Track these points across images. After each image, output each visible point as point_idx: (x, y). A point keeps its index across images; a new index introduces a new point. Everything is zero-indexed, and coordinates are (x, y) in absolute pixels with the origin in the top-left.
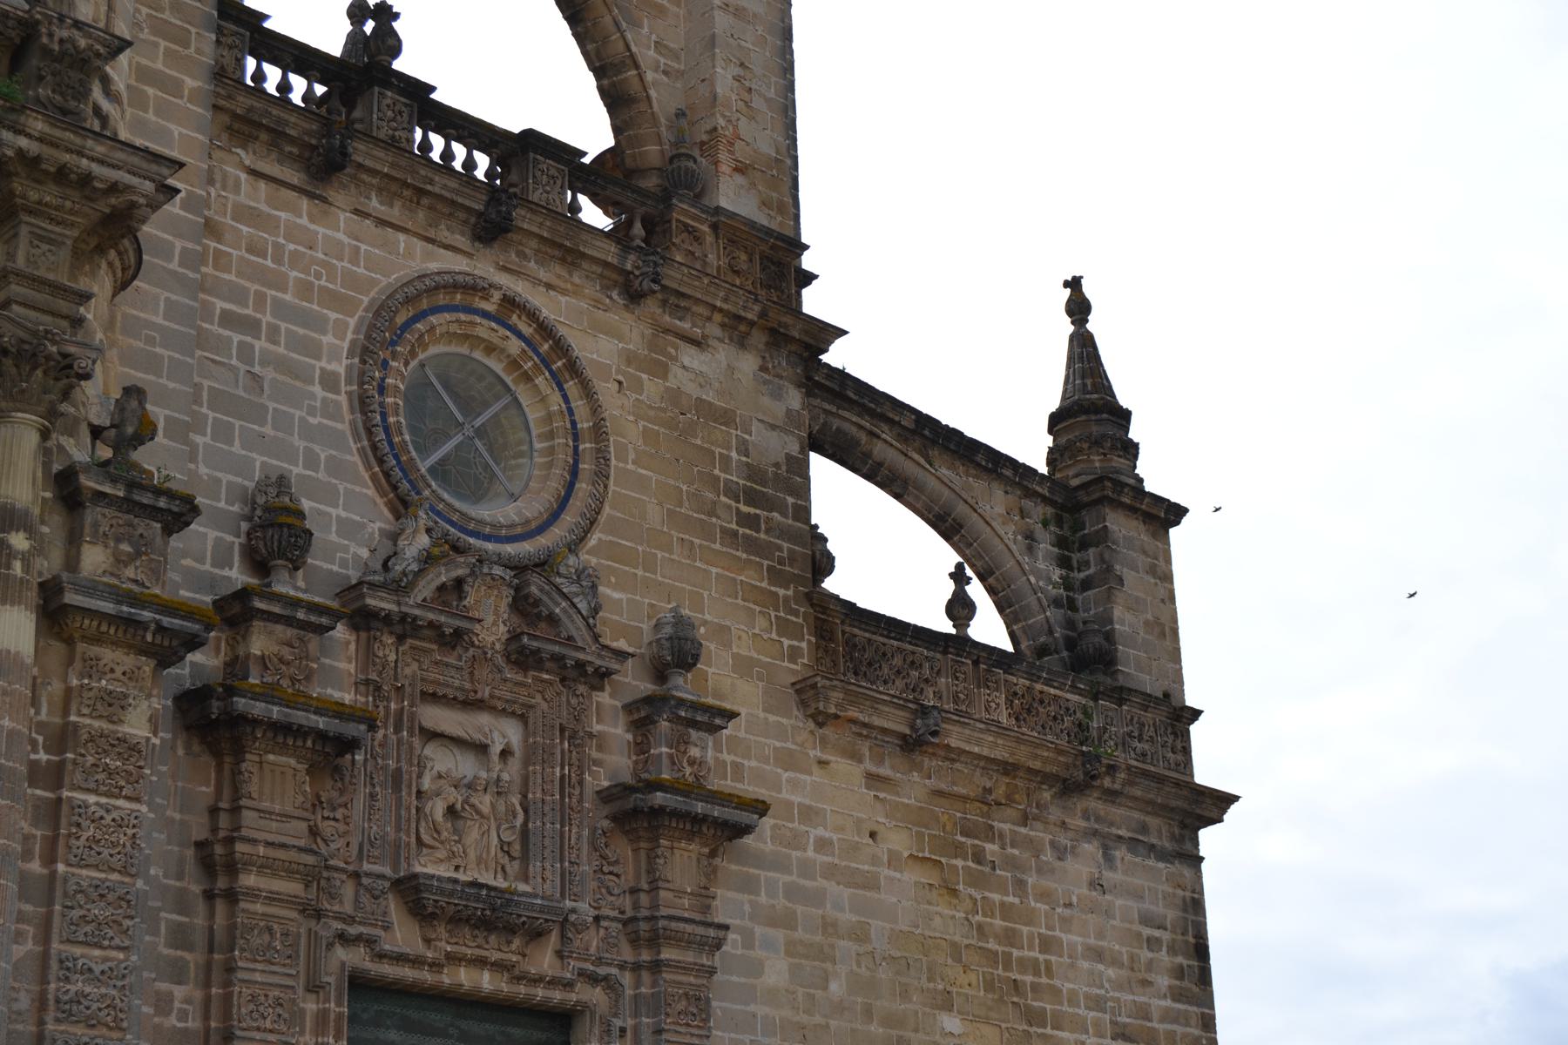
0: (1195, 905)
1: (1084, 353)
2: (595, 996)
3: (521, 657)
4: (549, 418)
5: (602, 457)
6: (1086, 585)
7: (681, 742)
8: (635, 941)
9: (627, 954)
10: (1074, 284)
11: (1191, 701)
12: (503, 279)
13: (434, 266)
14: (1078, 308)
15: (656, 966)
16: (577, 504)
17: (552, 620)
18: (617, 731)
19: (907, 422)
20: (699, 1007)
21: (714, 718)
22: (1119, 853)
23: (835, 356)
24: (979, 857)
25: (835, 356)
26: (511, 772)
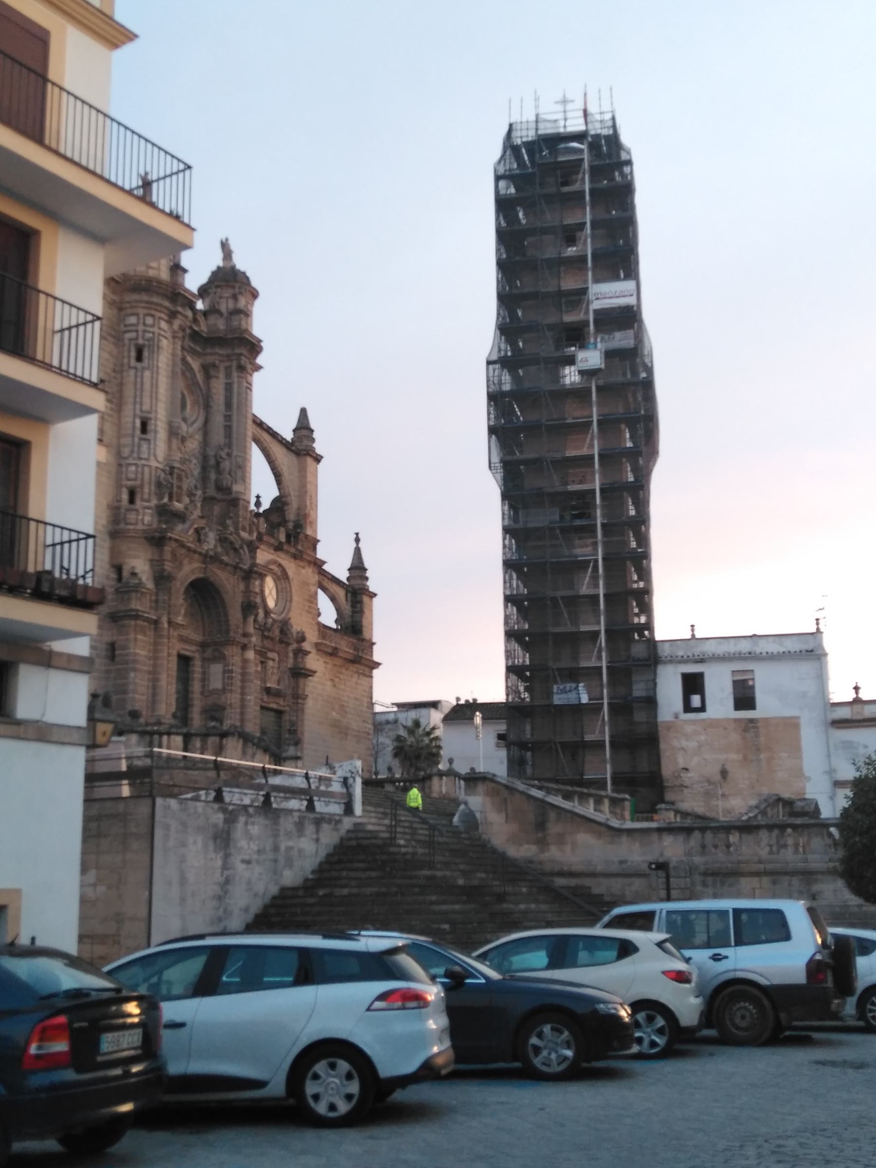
0: (371, 687)
1: (358, 552)
2: (287, 709)
3: (281, 641)
4: (283, 588)
5: (291, 597)
6: (357, 612)
7: (303, 658)
8: (293, 697)
9: (292, 701)
10: (357, 534)
11: (374, 641)
12: (279, 559)
13: (270, 558)
14: (357, 540)
15: (298, 703)
16: (287, 607)
17: (286, 634)
18: (291, 655)
19: (330, 577)
20: (303, 710)
21: (307, 653)
22: (361, 676)
23: (325, 567)
24: (339, 678)
25: (325, 567)
26: (276, 665)
